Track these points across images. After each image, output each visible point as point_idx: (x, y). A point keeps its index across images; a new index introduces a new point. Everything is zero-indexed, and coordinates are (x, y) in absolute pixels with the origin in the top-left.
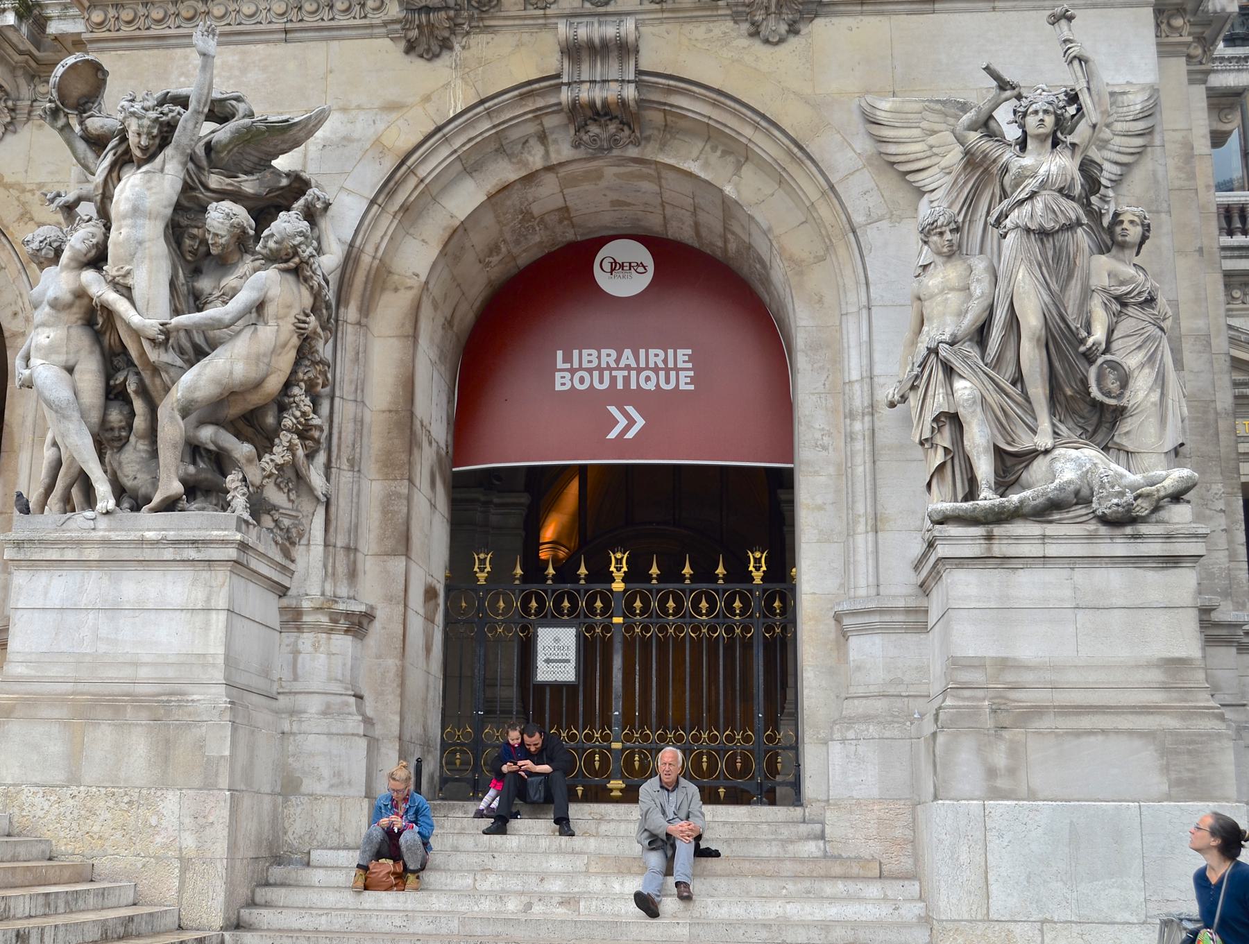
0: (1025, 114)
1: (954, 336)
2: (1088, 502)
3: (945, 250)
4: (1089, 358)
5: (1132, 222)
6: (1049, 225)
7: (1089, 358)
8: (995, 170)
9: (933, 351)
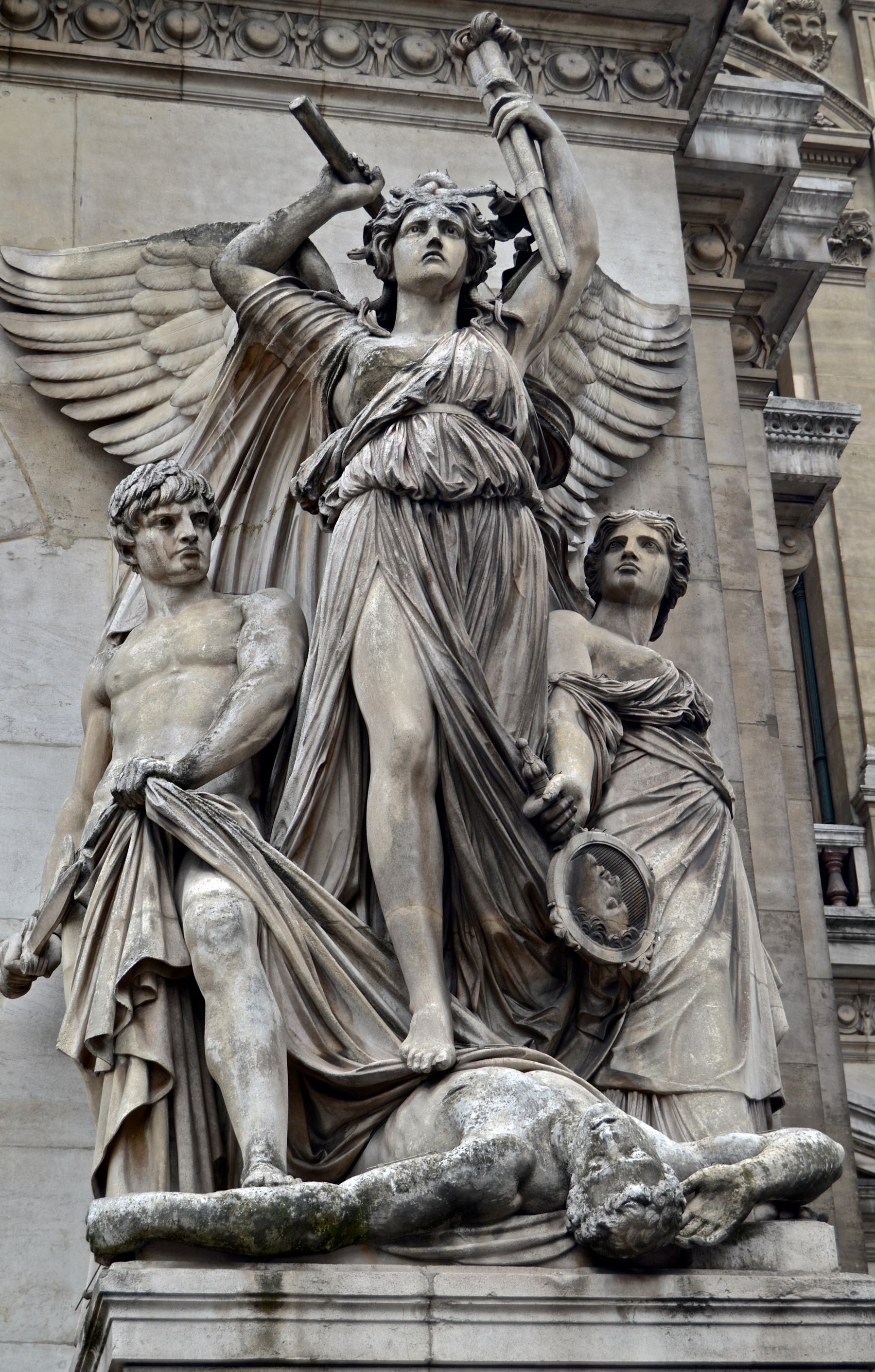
0: (393, 234)
1: (191, 762)
2: (552, 1204)
3: (177, 565)
4: (550, 830)
5: (645, 542)
6: (451, 481)
7: (550, 830)
8: (312, 370)
9: (130, 801)
